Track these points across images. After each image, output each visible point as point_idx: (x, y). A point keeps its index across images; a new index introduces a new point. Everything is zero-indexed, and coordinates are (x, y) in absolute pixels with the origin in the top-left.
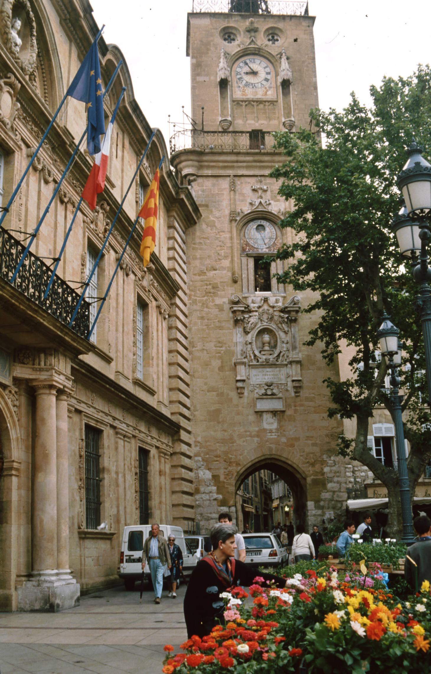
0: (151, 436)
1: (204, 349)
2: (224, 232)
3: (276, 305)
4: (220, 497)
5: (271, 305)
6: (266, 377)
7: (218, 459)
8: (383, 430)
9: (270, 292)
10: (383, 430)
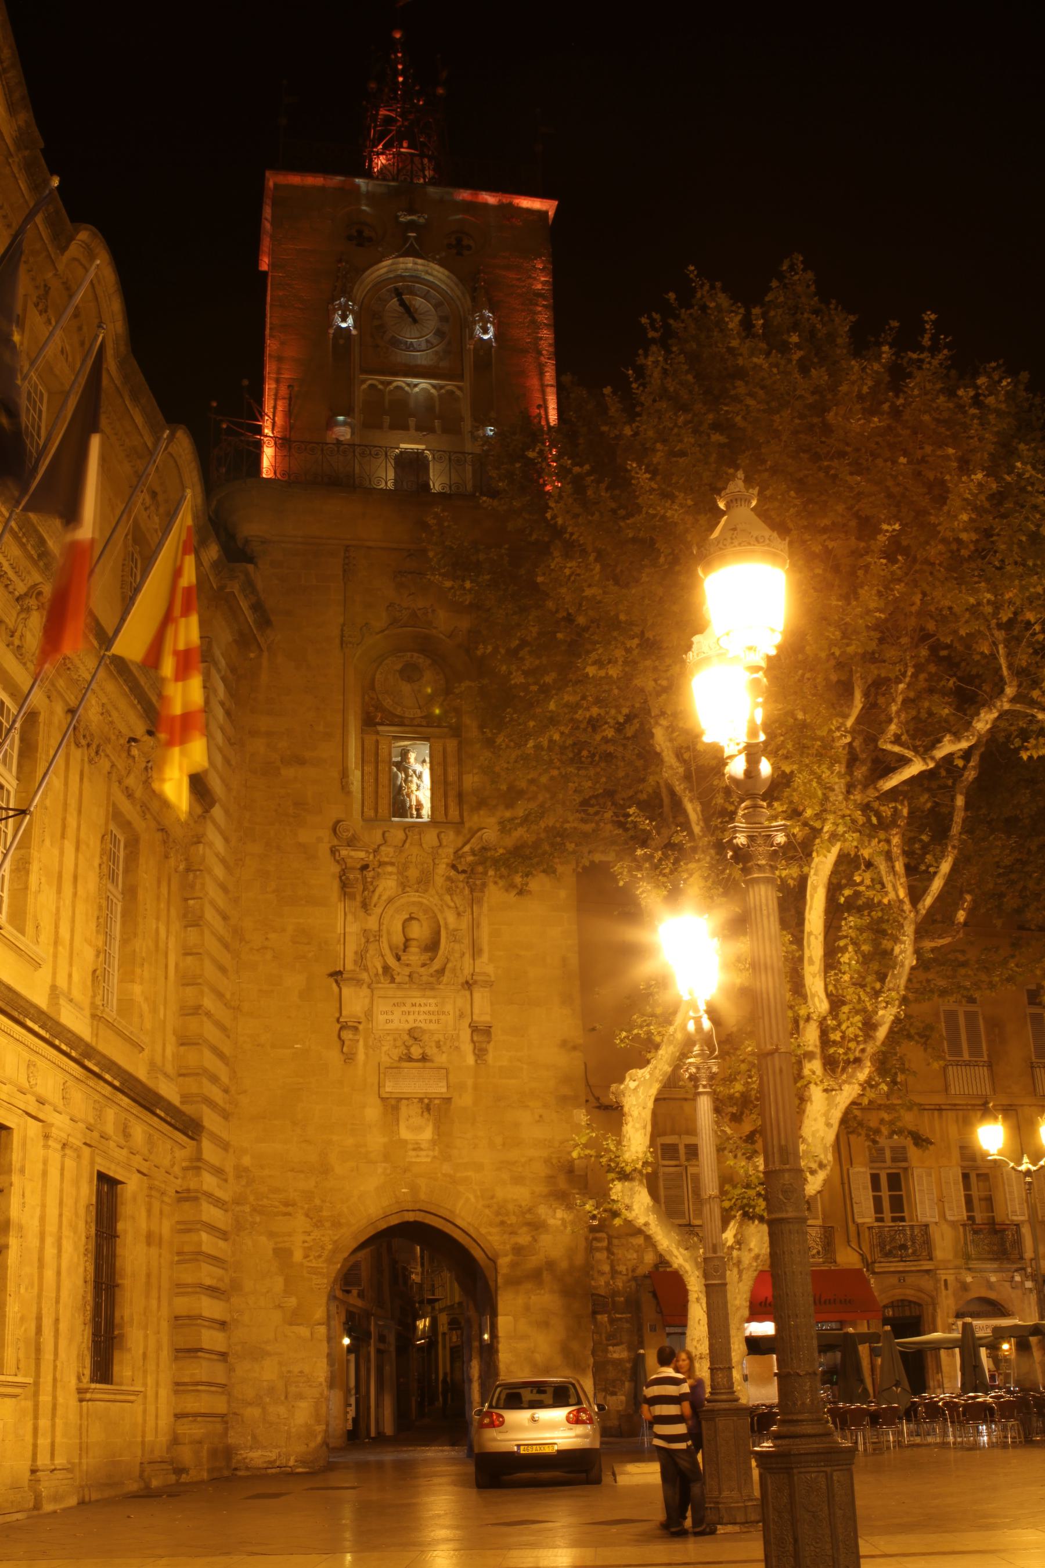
0: (130, 1148)
1: (265, 948)
4: (293, 1301)
6: (411, 1018)
7: (290, 1209)
8: (682, 1151)
10: (682, 1151)
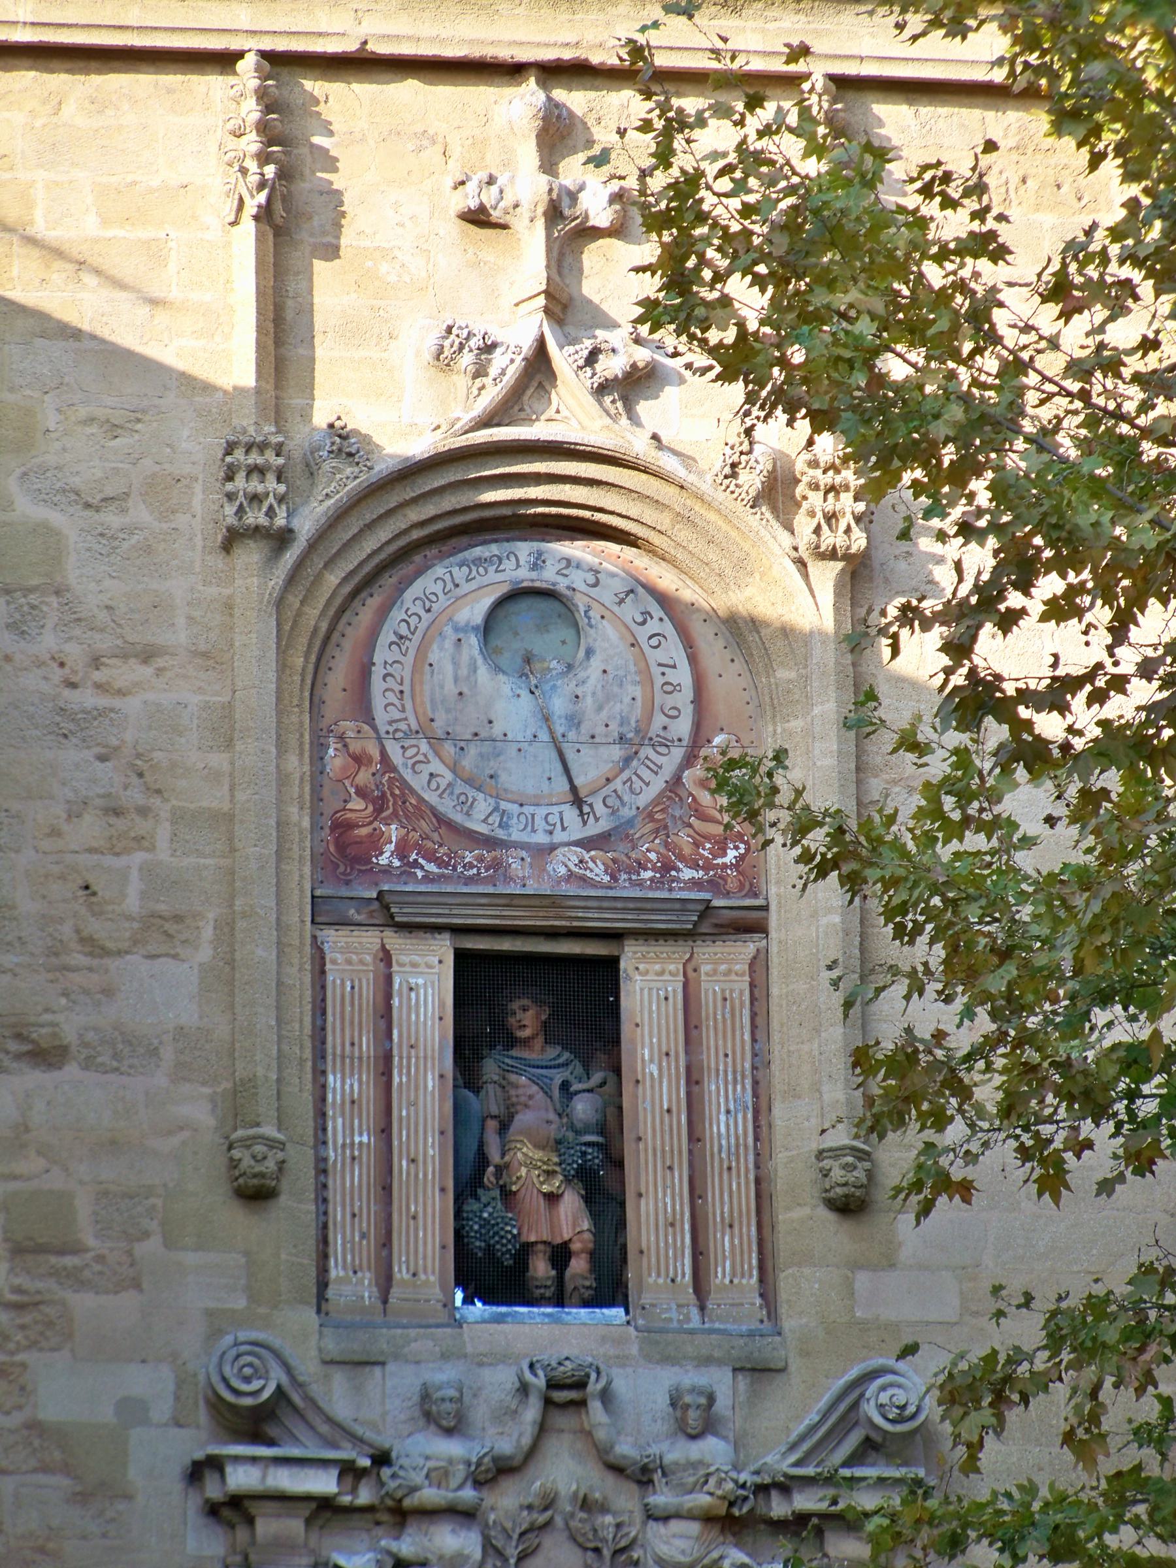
2: (147, 655)
3: (677, 1452)
5: (625, 1449)
9: (617, 1313)
